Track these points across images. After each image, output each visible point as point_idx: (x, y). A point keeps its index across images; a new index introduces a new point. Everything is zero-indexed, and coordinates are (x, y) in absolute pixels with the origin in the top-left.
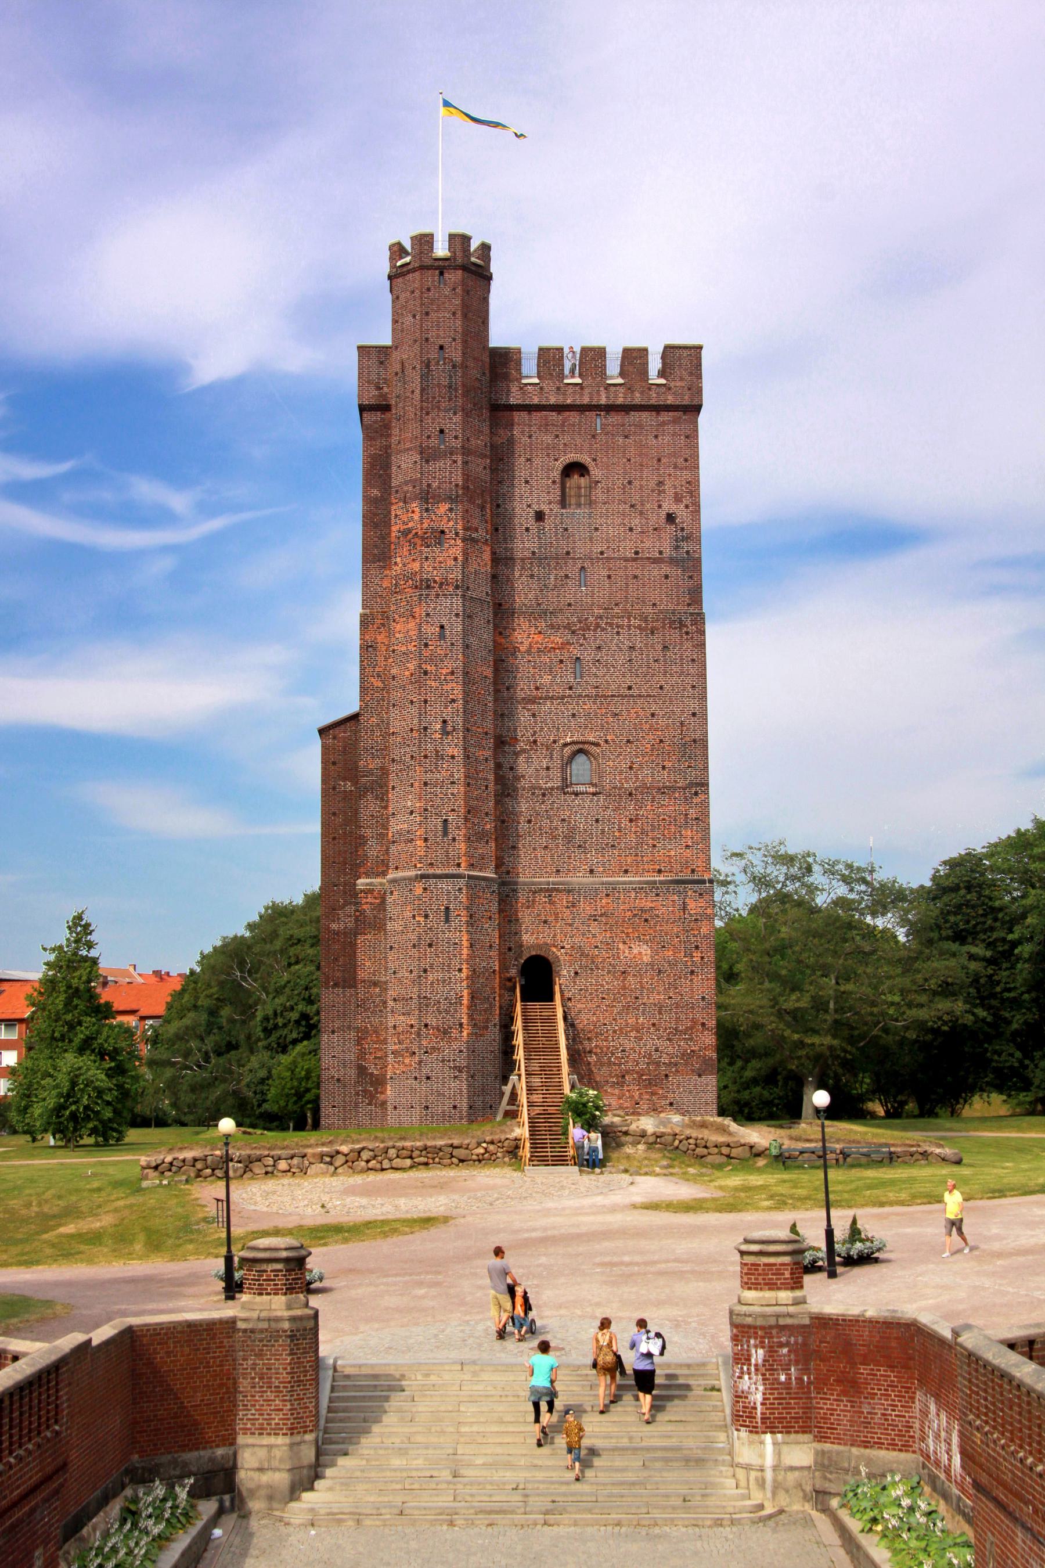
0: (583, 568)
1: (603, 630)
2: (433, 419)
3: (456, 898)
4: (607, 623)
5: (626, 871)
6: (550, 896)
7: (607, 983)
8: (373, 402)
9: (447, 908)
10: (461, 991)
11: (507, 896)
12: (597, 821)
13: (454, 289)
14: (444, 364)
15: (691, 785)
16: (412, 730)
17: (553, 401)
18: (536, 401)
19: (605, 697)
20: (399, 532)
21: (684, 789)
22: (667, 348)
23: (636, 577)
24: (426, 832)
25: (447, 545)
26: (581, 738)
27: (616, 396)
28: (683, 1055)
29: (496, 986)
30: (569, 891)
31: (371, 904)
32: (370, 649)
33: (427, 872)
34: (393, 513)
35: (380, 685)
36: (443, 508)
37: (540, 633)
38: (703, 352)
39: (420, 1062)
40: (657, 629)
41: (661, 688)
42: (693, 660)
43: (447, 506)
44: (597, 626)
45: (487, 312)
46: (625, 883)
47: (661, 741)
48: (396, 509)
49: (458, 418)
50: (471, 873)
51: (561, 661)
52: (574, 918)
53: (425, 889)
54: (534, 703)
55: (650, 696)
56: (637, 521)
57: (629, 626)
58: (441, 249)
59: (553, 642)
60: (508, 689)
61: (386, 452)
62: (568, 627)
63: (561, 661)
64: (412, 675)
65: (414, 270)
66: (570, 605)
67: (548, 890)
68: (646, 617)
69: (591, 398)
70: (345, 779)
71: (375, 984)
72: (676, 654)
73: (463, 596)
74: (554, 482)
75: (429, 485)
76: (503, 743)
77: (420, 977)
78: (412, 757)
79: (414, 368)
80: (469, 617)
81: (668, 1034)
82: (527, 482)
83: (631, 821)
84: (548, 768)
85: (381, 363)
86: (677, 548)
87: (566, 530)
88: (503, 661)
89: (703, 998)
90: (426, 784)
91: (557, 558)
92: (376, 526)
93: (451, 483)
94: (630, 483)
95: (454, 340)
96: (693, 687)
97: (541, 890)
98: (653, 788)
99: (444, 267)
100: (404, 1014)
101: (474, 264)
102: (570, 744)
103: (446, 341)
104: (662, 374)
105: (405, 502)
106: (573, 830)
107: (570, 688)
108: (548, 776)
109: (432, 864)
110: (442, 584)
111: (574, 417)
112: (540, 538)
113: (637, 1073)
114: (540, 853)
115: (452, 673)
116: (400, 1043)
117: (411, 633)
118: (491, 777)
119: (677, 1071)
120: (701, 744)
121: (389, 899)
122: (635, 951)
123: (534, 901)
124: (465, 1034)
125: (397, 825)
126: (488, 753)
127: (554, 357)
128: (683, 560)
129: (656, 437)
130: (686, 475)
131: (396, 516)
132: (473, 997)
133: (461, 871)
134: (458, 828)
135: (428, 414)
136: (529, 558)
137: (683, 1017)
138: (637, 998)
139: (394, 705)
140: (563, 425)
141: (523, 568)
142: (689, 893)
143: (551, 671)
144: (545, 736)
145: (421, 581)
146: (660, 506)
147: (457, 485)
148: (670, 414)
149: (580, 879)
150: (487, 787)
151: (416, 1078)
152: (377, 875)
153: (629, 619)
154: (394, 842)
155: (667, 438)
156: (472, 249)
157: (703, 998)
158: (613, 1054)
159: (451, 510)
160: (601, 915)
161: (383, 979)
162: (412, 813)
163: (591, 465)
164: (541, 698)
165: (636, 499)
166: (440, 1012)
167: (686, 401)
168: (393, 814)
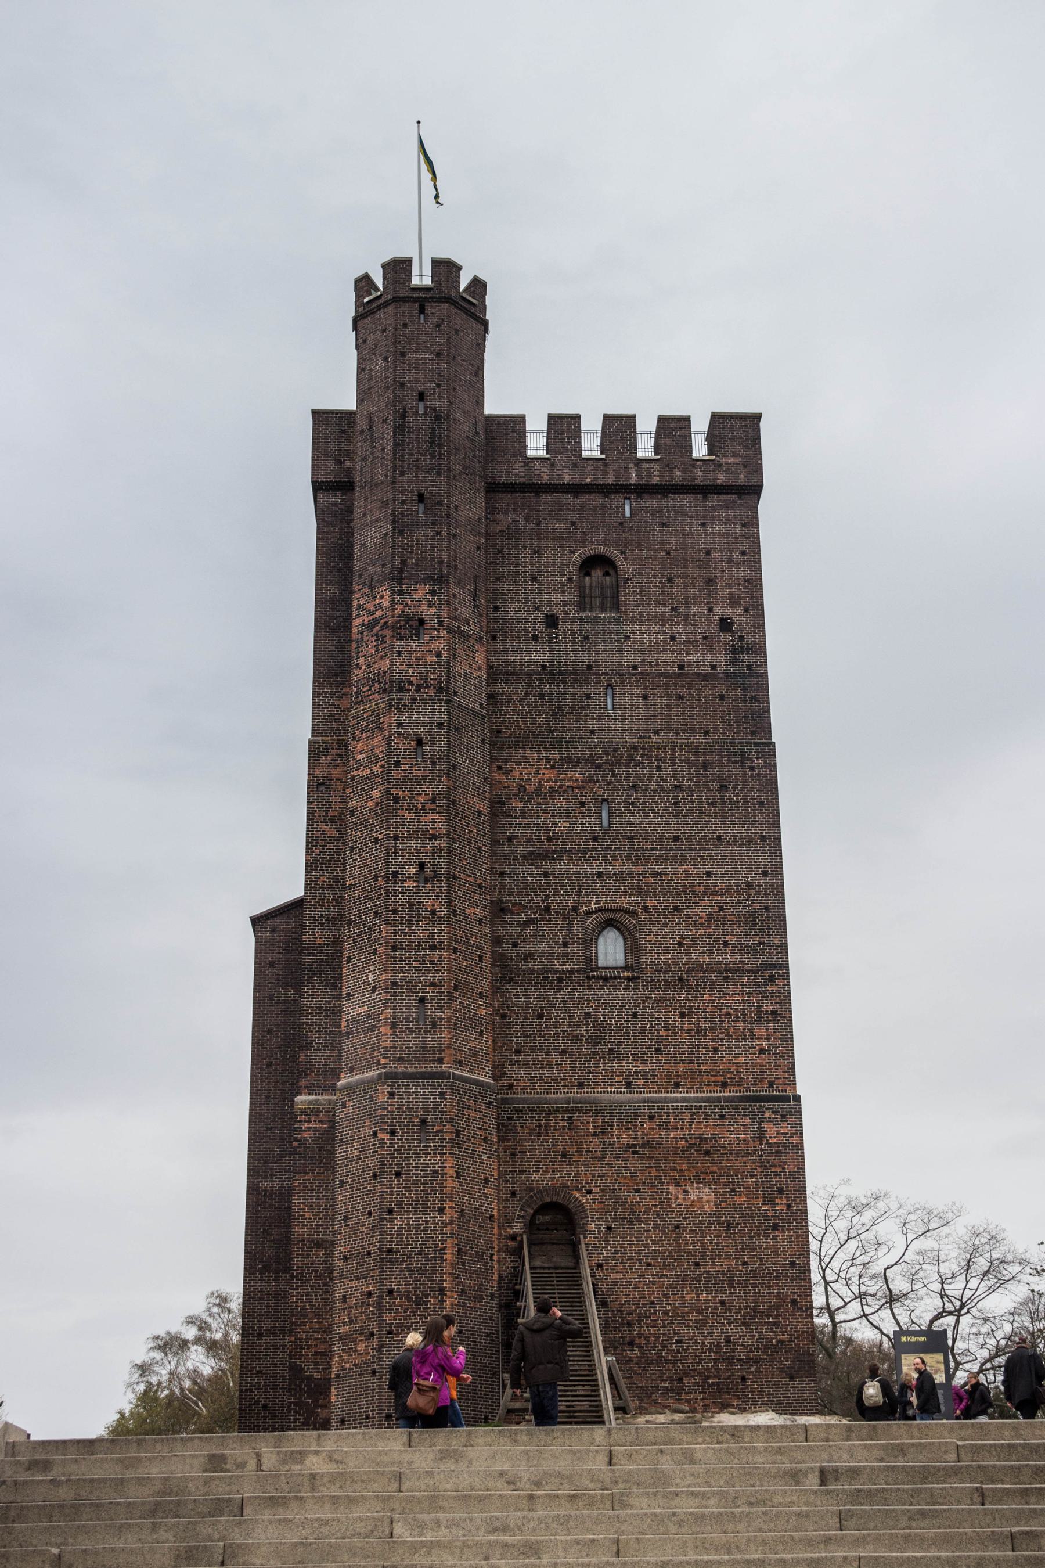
0: (609, 685)
1: (638, 764)
2: (410, 481)
3: (435, 1108)
4: (643, 756)
5: (677, 1085)
6: (570, 1118)
7: (654, 1242)
8: (331, 478)
9: (423, 1122)
10: (443, 1241)
11: (510, 1119)
12: (635, 1015)
13: (438, 326)
14: (425, 414)
15: (764, 967)
16: (376, 877)
17: (567, 479)
18: (546, 478)
19: (644, 850)
20: (363, 625)
21: (755, 972)
22: (717, 419)
23: (681, 698)
24: (394, 1015)
25: (427, 638)
26: (611, 905)
27: (650, 475)
28: (766, 1347)
29: (494, 1238)
30: (599, 1112)
31: (315, 1129)
32: (322, 788)
33: (394, 1070)
34: (355, 604)
35: (335, 833)
36: (422, 590)
37: (553, 767)
38: (763, 424)
39: (381, 1347)
40: (712, 763)
41: (719, 838)
42: (761, 803)
43: (428, 588)
44: (631, 758)
45: (482, 361)
46: (676, 1100)
47: (721, 909)
48: (358, 599)
50: (458, 1073)
51: (582, 804)
52: (604, 1150)
53: (392, 1095)
54: (545, 857)
55: (704, 849)
56: (681, 628)
57: (673, 760)
59: (571, 779)
60: (510, 839)
61: (348, 541)
62: (591, 760)
63: (582, 804)
64: (377, 804)
65: (386, 304)
66: (592, 732)
67: (567, 1110)
68: (697, 747)
69: (617, 477)
70: (286, 985)
71: (319, 1245)
72: (737, 795)
73: (448, 702)
74: (570, 580)
75: (404, 562)
76: (502, 910)
77: (382, 1220)
78: (376, 913)
79: (384, 421)
80: (457, 729)
81: (744, 1317)
82: (534, 579)
83: (682, 1015)
84: (565, 945)
85: (343, 432)
86: (734, 661)
87: (587, 638)
88: (503, 803)
89: (793, 1264)
90: (394, 948)
91: (576, 674)
92: (333, 631)
93: (433, 559)
95: (438, 385)
96: (763, 838)
97: (557, 1109)
98: (709, 970)
100: (358, 1278)
102: (596, 912)
105: (371, 587)
106: (602, 1028)
107: (595, 839)
108: (565, 955)
109: (401, 1059)
110: (419, 687)
111: (594, 500)
112: (552, 649)
113: (700, 1374)
115: (433, 801)
116: (351, 1322)
117: (377, 751)
118: (487, 946)
119: (758, 1371)
120: (777, 911)
121: (341, 1115)
122: (693, 1197)
123: (547, 1126)
124: (447, 1304)
125: (353, 1010)
126: (481, 913)
127: (569, 428)
128: (743, 676)
129: (703, 525)
130: (743, 571)
131: (359, 606)
132: (459, 1250)
133: (444, 1068)
134: (440, 1009)
135: (402, 473)
136: (539, 674)
137: (764, 1291)
138: (697, 1264)
139: (352, 848)
140: (581, 510)
141: (529, 685)
142: (767, 1115)
143: (568, 817)
144: (562, 902)
145: (391, 681)
146: (710, 610)
147: (441, 562)
148: (721, 497)
149: (613, 1095)
150: (481, 958)
151: (374, 1372)
152: (324, 1091)
153: (673, 750)
154: (348, 1034)
156: (461, 290)
157: (793, 1264)
158: (664, 1346)
159: (433, 593)
160: (643, 1146)
161: (329, 1238)
162: (374, 989)
163: (619, 560)
164: (555, 852)
165: (678, 598)
166: (411, 1272)
167: (742, 479)
168: (349, 995)
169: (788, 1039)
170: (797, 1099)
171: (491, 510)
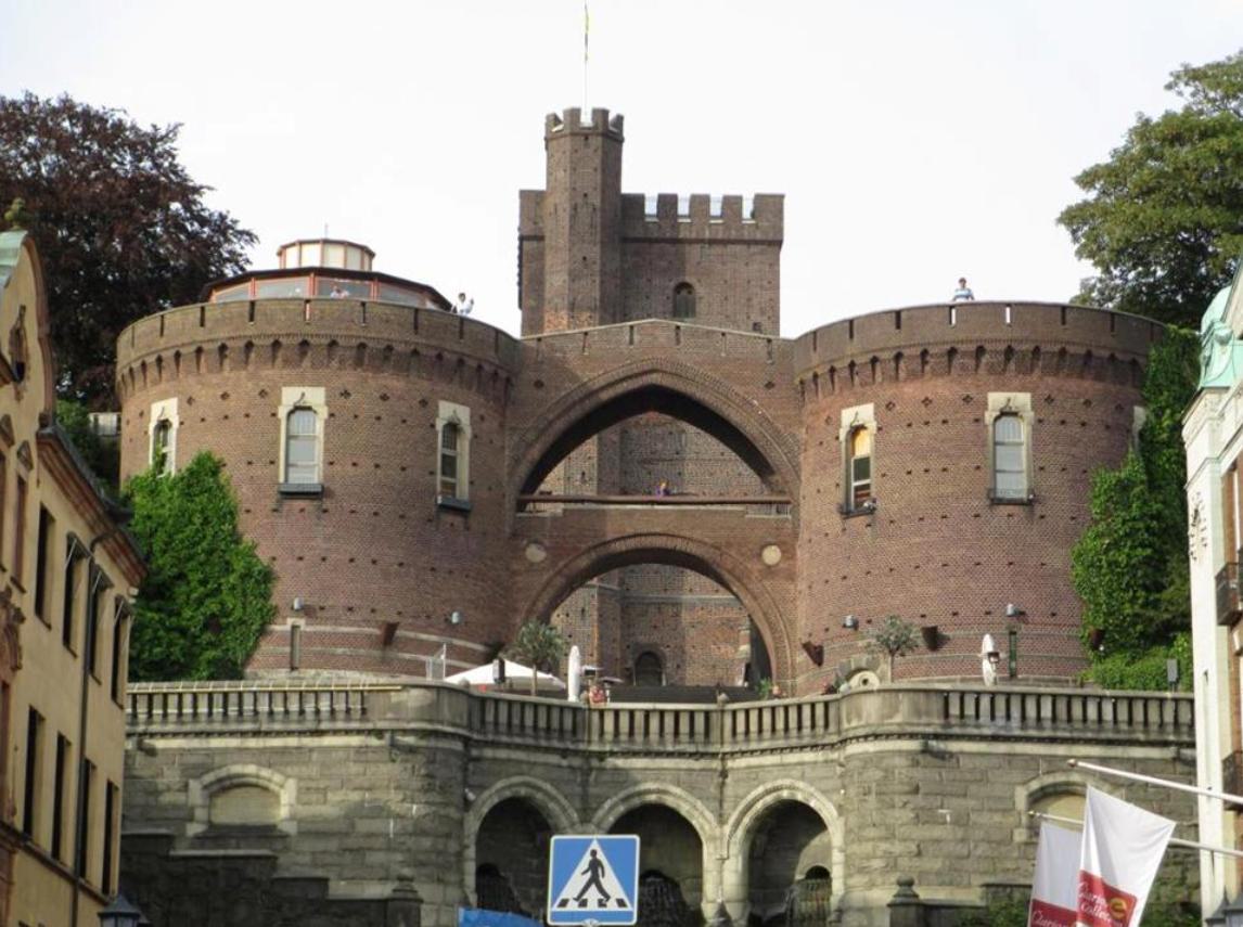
8: (532, 234)
9: (583, 611)
17: (668, 235)
18: (656, 235)
34: (546, 319)
38: (787, 203)
48: (547, 317)
49: (597, 249)
58: (586, 120)
65: (565, 136)
94: (726, 299)
103: (589, 191)
104: (753, 215)
105: (556, 311)
129: (747, 264)
146: (748, 317)
155: (756, 267)
167: (771, 237)
171: (624, 254)
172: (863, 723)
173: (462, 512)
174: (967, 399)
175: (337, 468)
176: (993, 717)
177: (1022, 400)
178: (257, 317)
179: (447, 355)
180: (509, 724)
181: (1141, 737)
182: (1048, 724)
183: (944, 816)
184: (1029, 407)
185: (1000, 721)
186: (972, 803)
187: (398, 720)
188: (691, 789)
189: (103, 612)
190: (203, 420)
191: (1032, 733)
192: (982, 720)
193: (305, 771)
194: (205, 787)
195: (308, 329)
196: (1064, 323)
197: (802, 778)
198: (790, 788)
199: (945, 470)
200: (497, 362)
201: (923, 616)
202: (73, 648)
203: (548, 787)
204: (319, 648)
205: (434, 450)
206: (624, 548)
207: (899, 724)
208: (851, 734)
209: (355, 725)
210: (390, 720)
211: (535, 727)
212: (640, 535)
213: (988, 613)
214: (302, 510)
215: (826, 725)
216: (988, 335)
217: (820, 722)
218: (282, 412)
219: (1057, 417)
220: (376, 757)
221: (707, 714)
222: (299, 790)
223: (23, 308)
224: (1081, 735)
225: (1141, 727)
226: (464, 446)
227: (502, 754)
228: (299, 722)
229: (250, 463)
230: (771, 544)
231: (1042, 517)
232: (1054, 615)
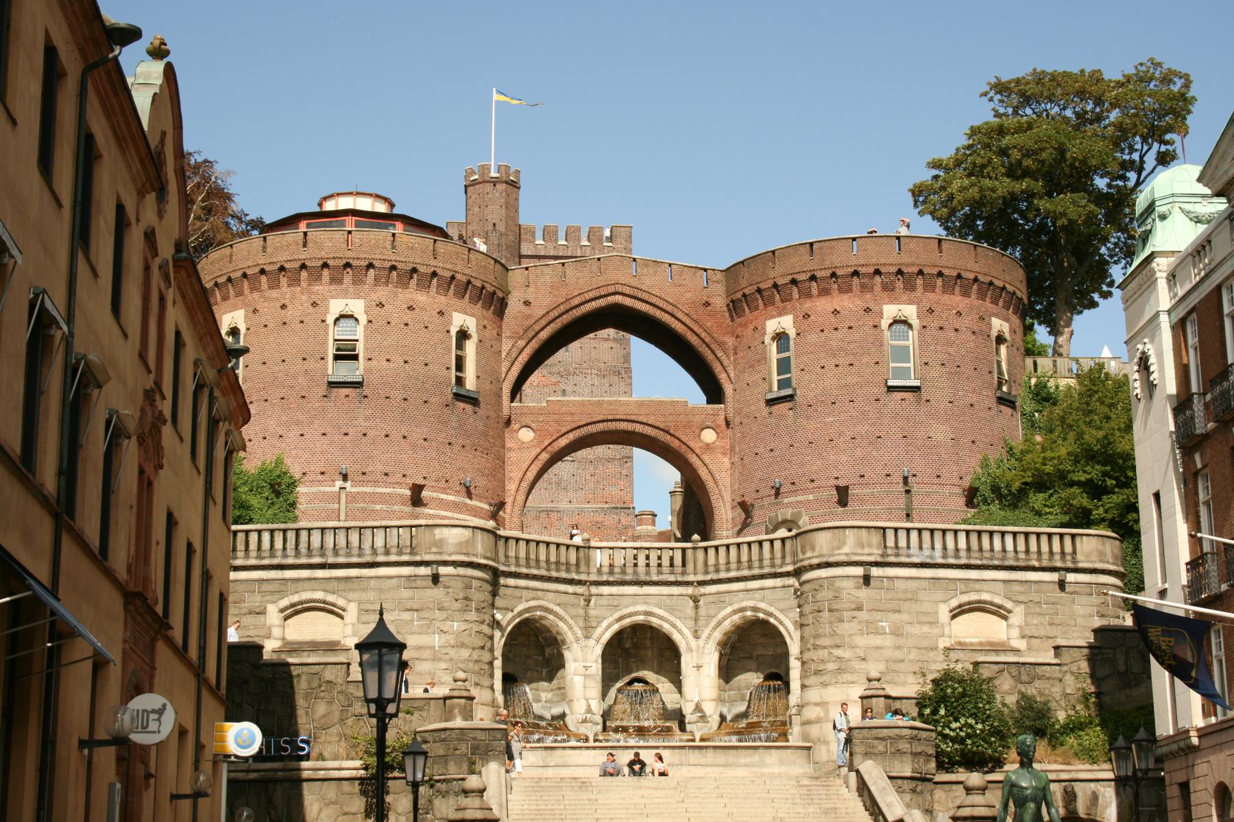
1: (578, 375)
5: (589, 502)
15: (624, 457)
18: (543, 254)
44: (575, 373)
63: (555, 391)
65: (480, 183)
67: (547, 511)
83: (592, 475)
99: (496, 182)
101: (512, 181)
114: (543, 491)
149: (563, 505)
169: (631, 485)
170: (634, 508)
172: (816, 554)
173: (473, 401)
174: (868, 310)
175: (374, 362)
176: (921, 548)
177: (910, 311)
178: (310, 245)
179: (458, 276)
180: (528, 559)
181: (1036, 564)
182: (963, 554)
183: (884, 628)
184: (915, 316)
185: (927, 552)
186: (905, 617)
187: (440, 553)
188: (671, 610)
189: (217, 439)
190: (266, 326)
191: (952, 561)
192: (912, 551)
193: (364, 596)
194: (282, 611)
195: (350, 254)
196: (941, 252)
197: (762, 600)
198: (755, 609)
199: (851, 365)
200: (495, 284)
201: (837, 478)
202: (197, 463)
203: (557, 609)
204: (362, 505)
205: (450, 351)
206: (595, 431)
207: (846, 554)
208: (806, 563)
209: (405, 558)
210: (436, 553)
211: (548, 561)
212: (607, 421)
213: (888, 475)
214: (347, 396)
215: (783, 557)
216: (882, 261)
217: (778, 555)
218: (330, 320)
219: (936, 324)
220: (424, 583)
221: (684, 550)
222: (360, 610)
223: (164, 134)
224: (990, 563)
225: (1035, 556)
226: (470, 347)
227: (522, 583)
228: (360, 555)
229: (304, 359)
230: (708, 427)
231: (928, 401)
232: (938, 476)
